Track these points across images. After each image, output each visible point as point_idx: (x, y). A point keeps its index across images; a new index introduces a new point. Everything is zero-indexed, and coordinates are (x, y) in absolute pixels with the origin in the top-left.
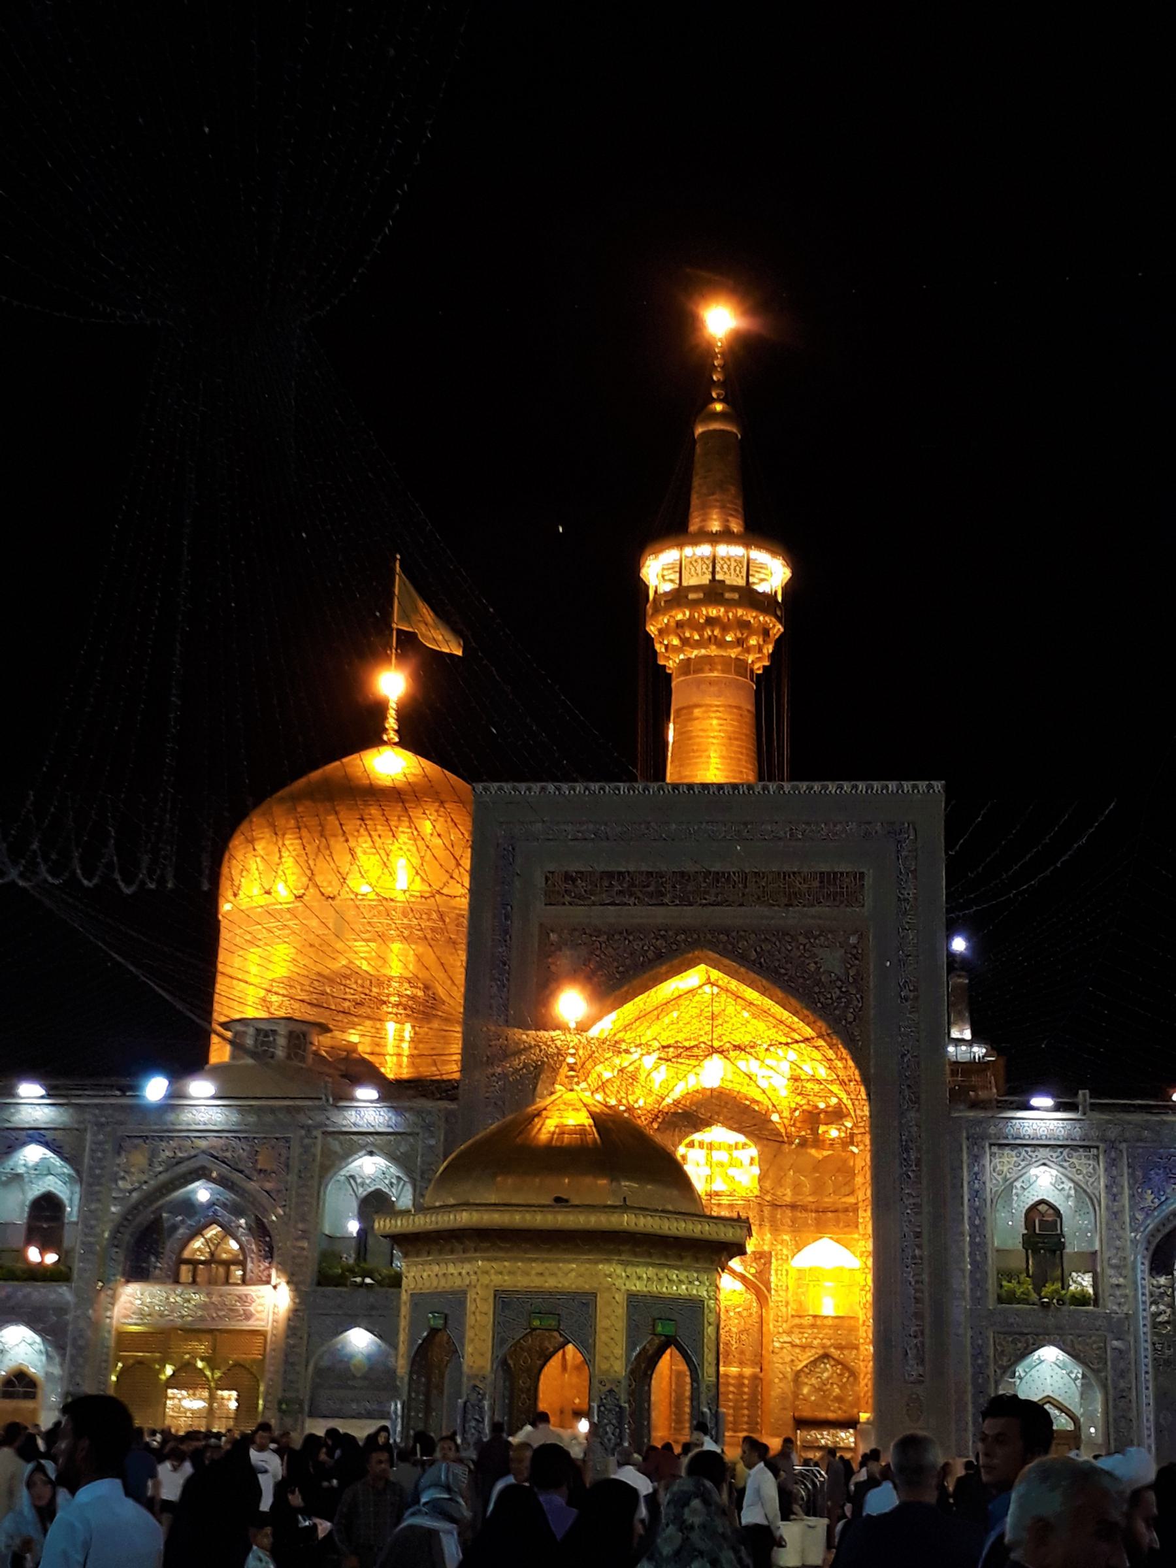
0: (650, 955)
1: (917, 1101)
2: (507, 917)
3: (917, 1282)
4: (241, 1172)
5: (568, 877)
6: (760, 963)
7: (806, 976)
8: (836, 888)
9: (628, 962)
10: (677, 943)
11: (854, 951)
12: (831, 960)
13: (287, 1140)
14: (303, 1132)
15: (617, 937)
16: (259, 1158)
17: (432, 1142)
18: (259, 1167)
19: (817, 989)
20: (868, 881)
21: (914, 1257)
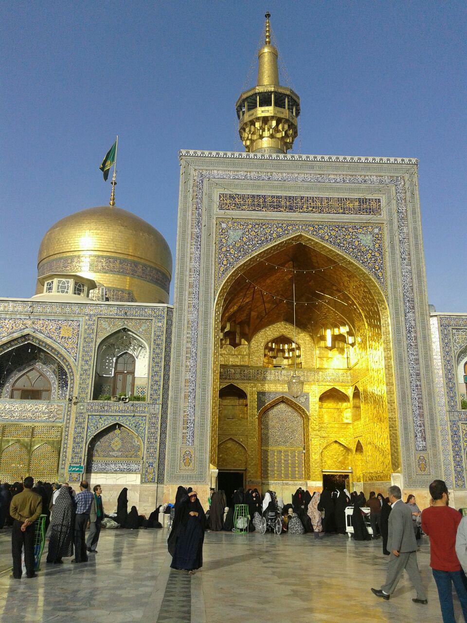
0: (274, 235)
1: (413, 308)
2: (199, 215)
3: (419, 398)
4: (51, 338)
5: (232, 197)
6: (331, 241)
7: (354, 247)
8: (367, 206)
9: (263, 238)
10: (288, 230)
11: (377, 236)
12: (366, 240)
13: (78, 321)
14: (87, 318)
15: (257, 226)
16: (61, 330)
17: (160, 324)
18: (61, 336)
19: (359, 254)
20: (383, 203)
21: (417, 386)
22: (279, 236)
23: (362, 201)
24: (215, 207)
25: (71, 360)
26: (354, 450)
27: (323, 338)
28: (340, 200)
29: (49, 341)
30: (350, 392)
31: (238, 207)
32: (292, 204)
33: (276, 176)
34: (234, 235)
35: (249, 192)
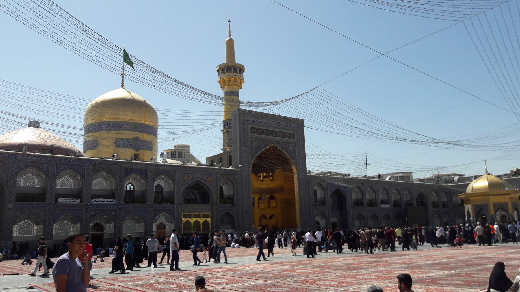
5: (254, 128)
8: (291, 136)
12: (291, 148)
22: (268, 145)
23: (290, 134)
24: (250, 132)
25: (212, 189)
26: (268, 217)
27: (260, 176)
28: (284, 133)
29: (204, 182)
30: (268, 196)
31: (256, 133)
32: (271, 133)
33: (267, 122)
34: (255, 143)
35: (258, 127)
